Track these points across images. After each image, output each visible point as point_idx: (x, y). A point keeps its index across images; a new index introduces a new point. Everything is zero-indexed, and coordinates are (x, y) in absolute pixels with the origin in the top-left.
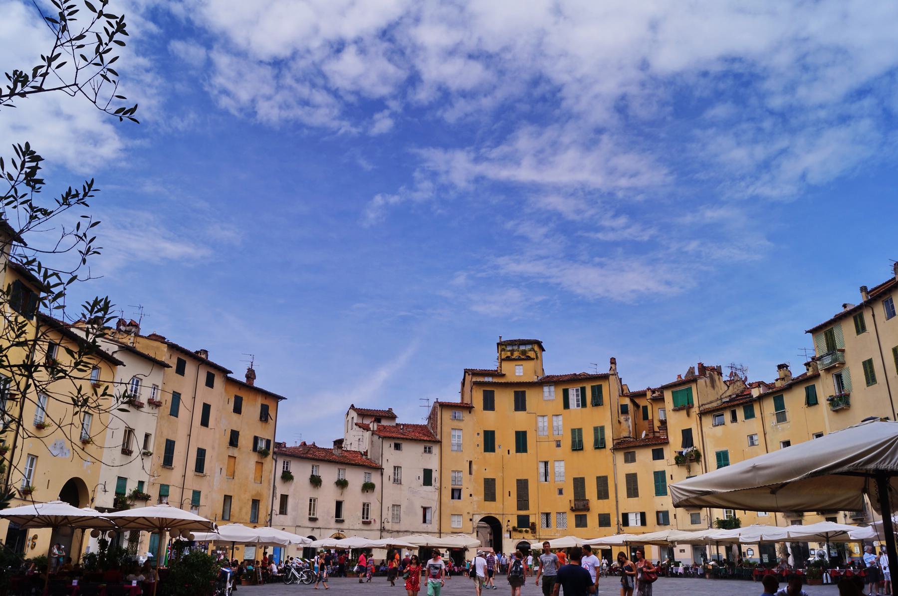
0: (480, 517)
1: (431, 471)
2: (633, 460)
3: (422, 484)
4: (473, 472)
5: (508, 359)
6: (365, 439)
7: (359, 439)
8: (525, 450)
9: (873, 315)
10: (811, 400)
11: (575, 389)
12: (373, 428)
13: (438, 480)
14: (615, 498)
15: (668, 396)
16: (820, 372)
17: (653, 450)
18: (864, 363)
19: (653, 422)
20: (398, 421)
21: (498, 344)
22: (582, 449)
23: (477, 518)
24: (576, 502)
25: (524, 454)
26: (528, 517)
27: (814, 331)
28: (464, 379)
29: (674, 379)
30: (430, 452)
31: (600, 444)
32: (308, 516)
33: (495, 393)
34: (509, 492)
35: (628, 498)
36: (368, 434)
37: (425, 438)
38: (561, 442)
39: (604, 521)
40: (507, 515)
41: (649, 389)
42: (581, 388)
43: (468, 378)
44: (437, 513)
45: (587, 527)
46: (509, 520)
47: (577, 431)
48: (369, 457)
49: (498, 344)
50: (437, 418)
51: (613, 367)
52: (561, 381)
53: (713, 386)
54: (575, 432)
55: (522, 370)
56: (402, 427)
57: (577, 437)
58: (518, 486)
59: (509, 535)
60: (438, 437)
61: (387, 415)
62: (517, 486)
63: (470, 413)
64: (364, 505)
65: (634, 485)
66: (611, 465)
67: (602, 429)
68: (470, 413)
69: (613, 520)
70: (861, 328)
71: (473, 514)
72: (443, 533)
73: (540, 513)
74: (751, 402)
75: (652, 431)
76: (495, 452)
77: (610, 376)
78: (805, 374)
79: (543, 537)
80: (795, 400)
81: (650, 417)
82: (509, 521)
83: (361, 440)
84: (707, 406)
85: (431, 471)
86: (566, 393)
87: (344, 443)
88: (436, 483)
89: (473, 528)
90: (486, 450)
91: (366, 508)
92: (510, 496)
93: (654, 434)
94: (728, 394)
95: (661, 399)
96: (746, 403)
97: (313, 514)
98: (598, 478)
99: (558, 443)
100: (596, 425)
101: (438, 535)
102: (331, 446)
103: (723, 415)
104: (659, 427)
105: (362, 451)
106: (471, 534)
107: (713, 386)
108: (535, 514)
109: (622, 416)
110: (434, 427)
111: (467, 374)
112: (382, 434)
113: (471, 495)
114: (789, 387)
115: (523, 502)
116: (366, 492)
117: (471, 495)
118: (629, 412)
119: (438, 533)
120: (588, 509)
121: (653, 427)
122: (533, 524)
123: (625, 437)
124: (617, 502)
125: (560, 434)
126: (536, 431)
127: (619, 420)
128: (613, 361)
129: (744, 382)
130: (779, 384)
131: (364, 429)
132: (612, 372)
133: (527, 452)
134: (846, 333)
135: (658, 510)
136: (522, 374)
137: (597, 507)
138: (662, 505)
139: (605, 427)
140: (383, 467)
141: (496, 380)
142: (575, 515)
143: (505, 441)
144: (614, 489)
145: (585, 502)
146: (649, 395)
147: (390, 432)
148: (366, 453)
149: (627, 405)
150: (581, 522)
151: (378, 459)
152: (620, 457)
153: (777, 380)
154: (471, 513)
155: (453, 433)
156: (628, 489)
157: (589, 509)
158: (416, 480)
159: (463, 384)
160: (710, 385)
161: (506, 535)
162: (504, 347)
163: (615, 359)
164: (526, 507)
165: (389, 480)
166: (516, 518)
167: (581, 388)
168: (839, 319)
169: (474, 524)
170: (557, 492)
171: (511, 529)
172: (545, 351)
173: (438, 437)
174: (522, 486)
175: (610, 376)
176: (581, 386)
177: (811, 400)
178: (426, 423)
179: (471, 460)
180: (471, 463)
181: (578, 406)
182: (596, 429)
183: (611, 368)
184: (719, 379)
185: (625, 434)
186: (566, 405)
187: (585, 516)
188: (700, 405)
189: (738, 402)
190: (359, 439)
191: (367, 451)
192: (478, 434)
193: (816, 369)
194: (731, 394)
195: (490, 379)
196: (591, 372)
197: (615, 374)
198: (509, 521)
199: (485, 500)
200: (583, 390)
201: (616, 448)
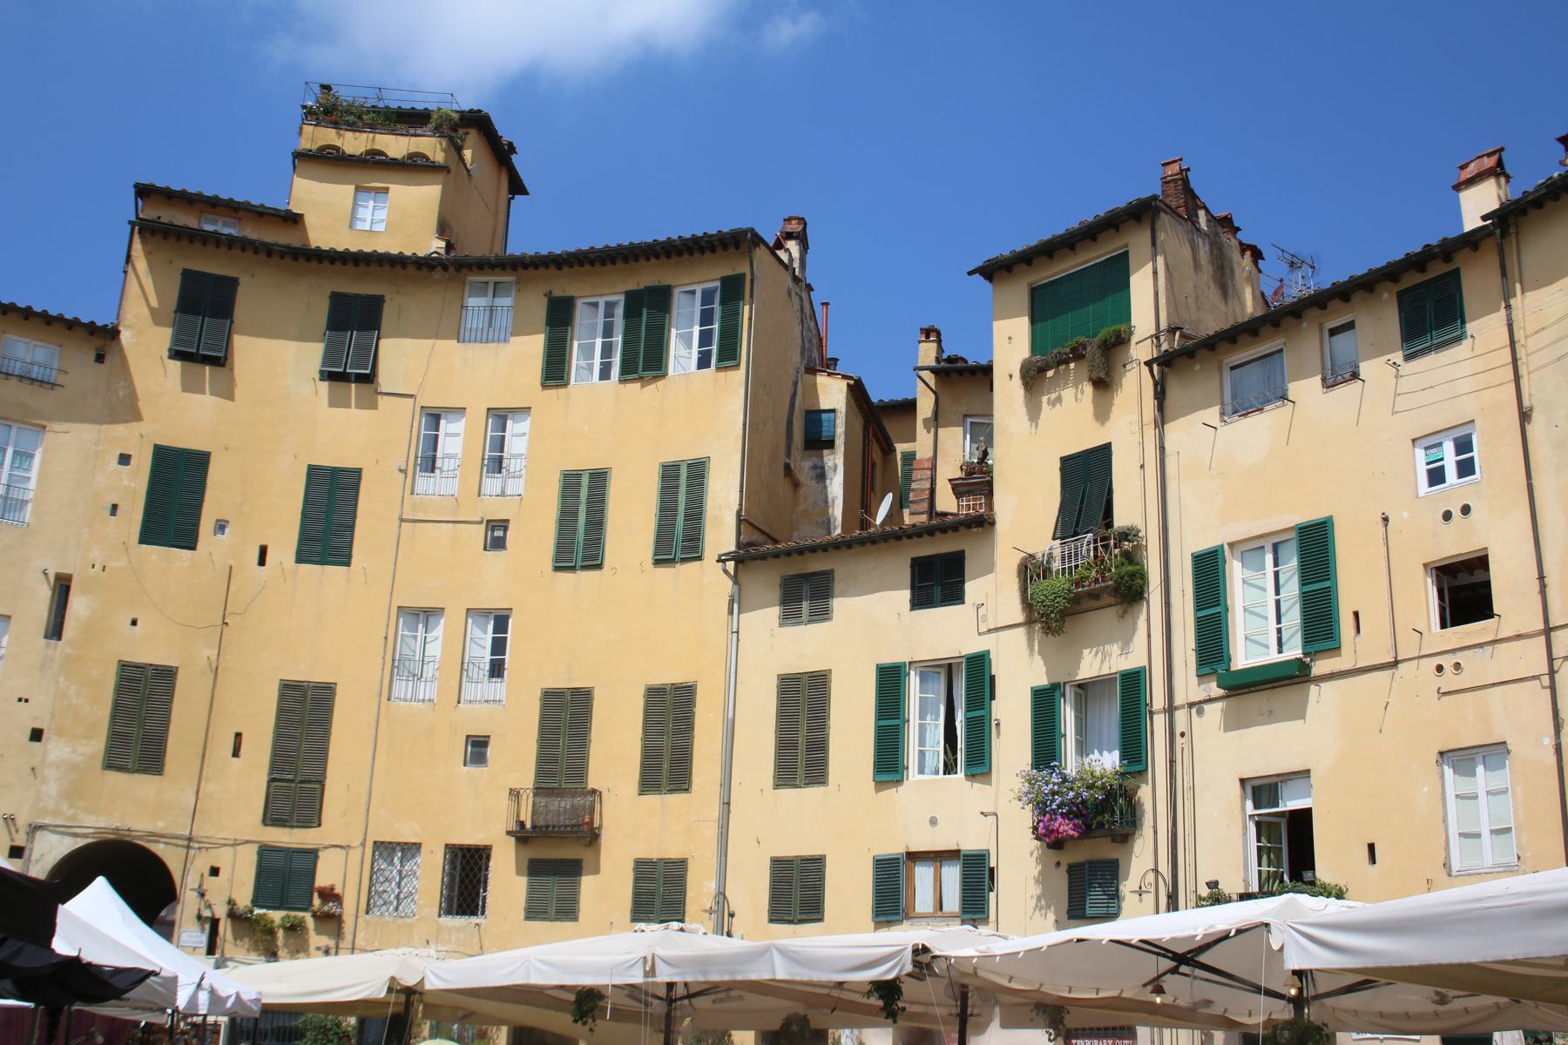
2: (822, 614)
4: (69, 630)
8: (342, 556)
11: (602, 301)
14: (714, 792)
19: (934, 468)
24: (543, 801)
25: (334, 572)
26: (312, 854)
33: (240, 290)
34: (238, 736)
35: (777, 786)
38: (511, 526)
45: (576, 919)
47: (585, 481)
54: (579, 484)
55: (382, 214)
58: (282, 712)
59: (202, 939)
62: (281, 711)
63: (100, 358)
65: (810, 730)
67: (698, 471)
68: (100, 358)
69: (699, 890)
71: (35, 828)
75: (925, 505)
76: (193, 547)
77: (762, 247)
86: (559, 317)
92: (236, 753)
98: (655, 695)
99: (499, 533)
100: (670, 458)
103: (1281, 351)
109: (802, 459)
113: (37, 735)
117: (37, 735)
118: (840, 442)
120: (592, 837)
122: (329, 895)
125: (508, 492)
127: (787, 468)
133: (348, 564)
135: (913, 849)
136: (380, 227)
138: (933, 821)
145: (579, 800)
154: (22, 822)
156: (785, 747)
160: (1210, 268)
163: (802, 221)
164: (310, 814)
166: (255, 858)
170: (459, 749)
171: (221, 911)
172: (527, 194)
175: (763, 247)
176: (632, 286)
179: (67, 571)
180: (62, 587)
181: (605, 374)
182: (669, 473)
186: (555, 371)
188: (1163, 326)
192: (125, 459)
198: (215, 872)
201: (744, 558)
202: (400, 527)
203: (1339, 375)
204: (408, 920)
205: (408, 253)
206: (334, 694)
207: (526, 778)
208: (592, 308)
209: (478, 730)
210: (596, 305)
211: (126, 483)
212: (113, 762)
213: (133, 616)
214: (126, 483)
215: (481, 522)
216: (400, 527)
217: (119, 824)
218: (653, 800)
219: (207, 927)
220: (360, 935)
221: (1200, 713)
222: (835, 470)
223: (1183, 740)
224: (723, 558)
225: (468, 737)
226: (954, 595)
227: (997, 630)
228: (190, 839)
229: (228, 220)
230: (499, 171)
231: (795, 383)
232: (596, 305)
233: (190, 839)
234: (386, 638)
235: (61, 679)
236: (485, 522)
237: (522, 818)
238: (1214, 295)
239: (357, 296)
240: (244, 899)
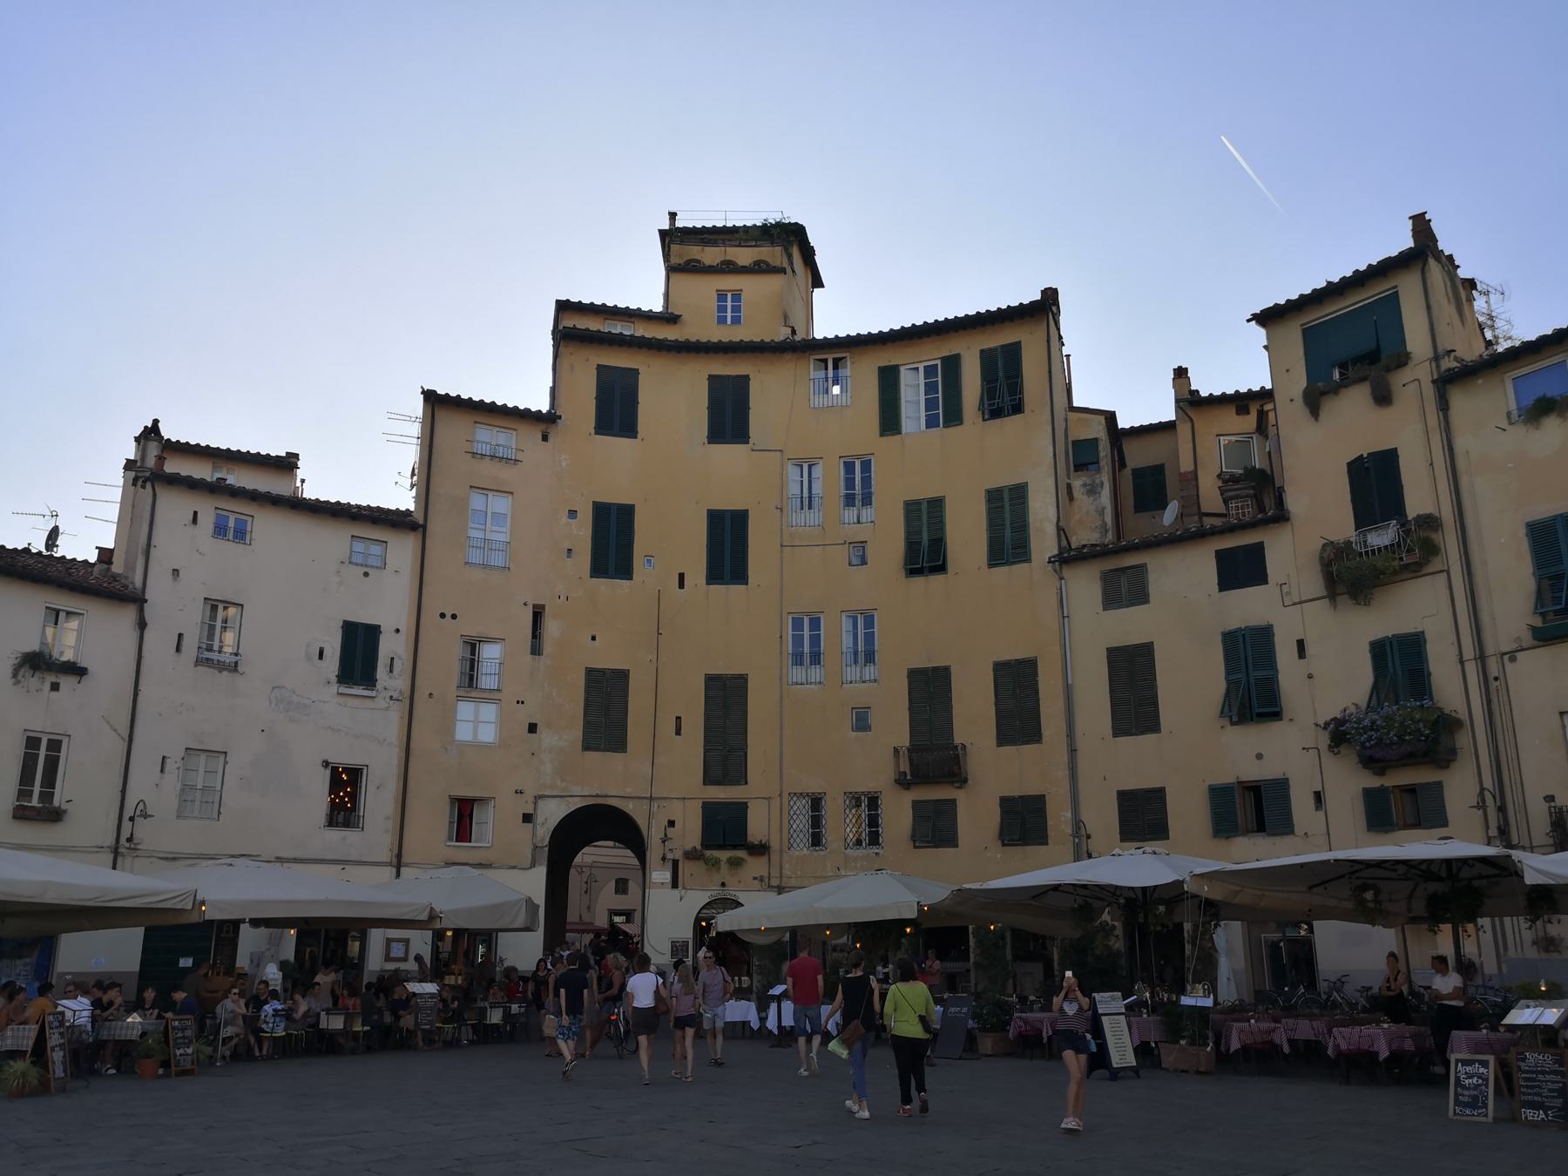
1: (373, 632)
2: (1139, 596)
3: (334, 679)
4: (548, 647)
8: (739, 575)
11: (921, 367)
17: (1221, 556)
19: (1196, 479)
21: (663, 234)
22: (941, 568)
23: (553, 813)
25: (736, 590)
34: (678, 718)
40: (663, 803)
42: (944, 360)
47: (924, 507)
49: (663, 234)
54: (920, 510)
57: (925, 529)
63: (545, 438)
64: (32, 743)
67: (1019, 493)
68: (545, 438)
69: (1059, 818)
71: (537, 798)
72: (407, 865)
73: (786, 796)
79: (793, 882)
82: (672, 823)
85: (373, 632)
86: (889, 380)
88: (390, 681)
89: (536, 847)
90: (600, 568)
92: (678, 732)
93: (1201, 519)
98: (1001, 669)
101: (389, 872)
106: (525, 869)
108: (769, 799)
113: (532, 728)
116: (47, 686)
117: (532, 728)
118: (1102, 463)
119: (390, 864)
121: (1198, 496)
124: (1073, 751)
125: (863, 519)
126: (781, 510)
133: (747, 584)
138: (1259, 756)
142: (916, 804)
144: (1060, 704)
149: (1096, 440)
154: (530, 793)
155: (477, 501)
157: (965, 781)
158: (309, 658)
164: (742, 779)
165: (178, 649)
166: (700, 811)
167: (944, 360)
171: (678, 855)
172: (821, 285)
176: (946, 353)
180: (538, 615)
181: (931, 422)
186: (890, 421)
187: (953, 802)
192: (573, 514)
198: (672, 823)
200: (952, 365)
201: (1068, 557)
202: (782, 551)
204: (822, 853)
205: (767, 340)
206: (746, 681)
207: (904, 740)
208: (915, 371)
210: (917, 369)
211: (575, 532)
212: (588, 746)
213: (594, 633)
214: (575, 532)
215: (845, 542)
216: (782, 551)
217: (597, 792)
218: (1008, 750)
219: (671, 863)
220: (786, 866)
221: (1513, 659)
222: (1102, 487)
223: (1498, 683)
224: (1052, 559)
225: (852, 708)
227: (1301, 603)
228: (651, 799)
229: (624, 323)
230: (806, 269)
231: (1066, 420)
232: (917, 369)
233: (651, 799)
234: (781, 637)
235: (546, 685)
236: (847, 545)
237: (902, 770)
239: (728, 376)
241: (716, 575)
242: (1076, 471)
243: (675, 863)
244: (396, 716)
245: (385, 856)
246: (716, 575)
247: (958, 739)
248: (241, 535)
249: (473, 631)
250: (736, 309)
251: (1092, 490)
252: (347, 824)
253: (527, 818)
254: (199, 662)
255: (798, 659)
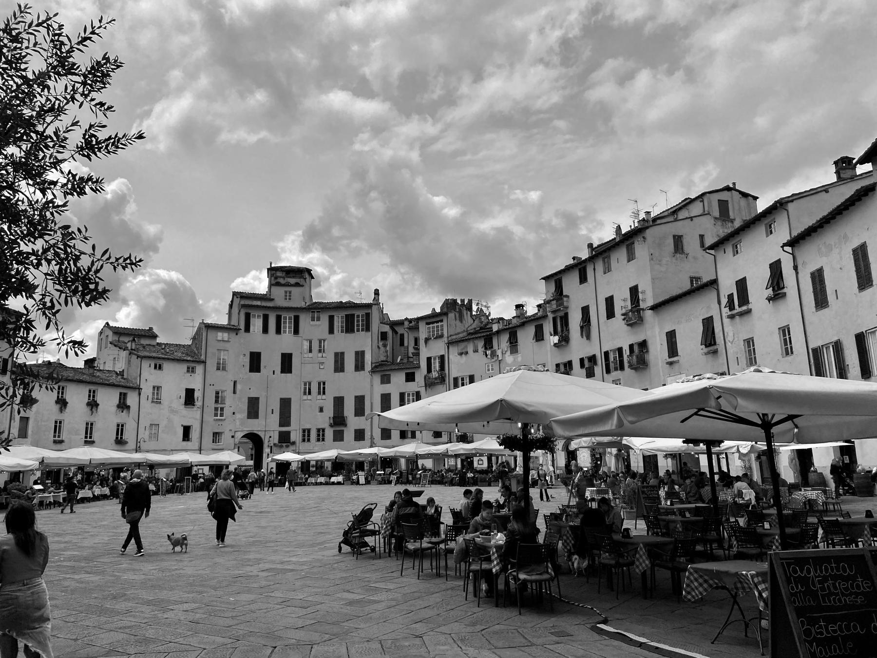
0: (243, 434)
1: (193, 390)
2: (389, 382)
4: (238, 392)
5: (278, 284)
6: (121, 358)
7: (115, 358)
8: (290, 371)
9: (594, 269)
10: (539, 336)
12: (131, 347)
13: (200, 399)
15: (422, 326)
16: (549, 314)
17: (406, 373)
18: (583, 308)
20: (158, 340)
21: (268, 269)
23: (239, 435)
26: (289, 433)
27: (547, 278)
28: (232, 301)
29: (429, 312)
30: (193, 372)
31: (359, 366)
32: (52, 438)
36: (124, 354)
37: (189, 358)
39: (360, 435)
41: (406, 319)
42: (346, 315)
43: (237, 301)
44: (198, 430)
46: (270, 436)
48: (125, 377)
50: (202, 338)
51: (377, 298)
52: (328, 308)
53: (461, 321)
56: (163, 347)
59: (269, 450)
60: (203, 357)
61: (147, 334)
63: (237, 334)
64: (118, 425)
66: (369, 386)
68: (237, 334)
69: (367, 435)
70: (583, 279)
71: (235, 432)
73: (301, 430)
74: (490, 335)
78: (537, 314)
79: (302, 451)
80: (526, 336)
81: (406, 344)
82: (270, 437)
83: (116, 359)
84: (454, 337)
85: (193, 390)
86: (331, 319)
87: (96, 362)
88: (198, 403)
89: (235, 444)
90: (251, 370)
91: (120, 429)
92: (272, 413)
93: (408, 359)
94: (474, 326)
95: (416, 328)
96: (487, 335)
97: (59, 437)
98: (356, 397)
100: (357, 350)
102: (81, 365)
104: (412, 353)
105: (118, 370)
107: (461, 321)
110: (199, 348)
111: (235, 297)
112: (141, 354)
113: (234, 413)
114: (523, 325)
115: (285, 418)
117: (234, 413)
120: (345, 425)
123: (382, 361)
128: (377, 292)
129: (487, 317)
130: (515, 321)
131: (120, 348)
132: (375, 302)
133: (291, 373)
134: (571, 284)
137: (354, 422)
139: (366, 352)
140: (141, 387)
141: (264, 304)
142: (334, 431)
143: (271, 362)
146: (406, 323)
147: (150, 351)
148: (122, 373)
149: (386, 332)
150: (339, 437)
151: (136, 379)
152: (377, 379)
153: (514, 318)
154: (233, 431)
158: (177, 398)
159: (231, 306)
161: (267, 450)
162: (273, 272)
164: (289, 425)
167: (346, 315)
168: (568, 269)
169: (236, 440)
170: (318, 410)
171: (272, 445)
173: (203, 357)
174: (286, 404)
177: (539, 336)
178: (190, 343)
180: (235, 383)
181: (342, 332)
182: (357, 353)
183: (375, 298)
184: (467, 314)
185: (384, 359)
186: (331, 331)
189: (479, 335)
190: (115, 358)
191: (123, 370)
193: (545, 311)
194: (475, 327)
195: (258, 303)
196: (357, 302)
197: (378, 304)
198: (270, 437)
199: (248, 418)
201: (373, 371)
203: (476, 351)
209: (321, 405)
218: (357, 418)
226: (413, 380)
238: (458, 322)
240: (276, 441)
241: (283, 371)
242: (382, 339)
243: (271, 447)
244: (199, 412)
245: (197, 447)
246: (283, 371)
247: (345, 414)
248: (160, 368)
249: (218, 389)
250: (290, 296)
251: (385, 346)
252: (188, 440)
253: (233, 437)
254: (152, 402)
255: (305, 393)
